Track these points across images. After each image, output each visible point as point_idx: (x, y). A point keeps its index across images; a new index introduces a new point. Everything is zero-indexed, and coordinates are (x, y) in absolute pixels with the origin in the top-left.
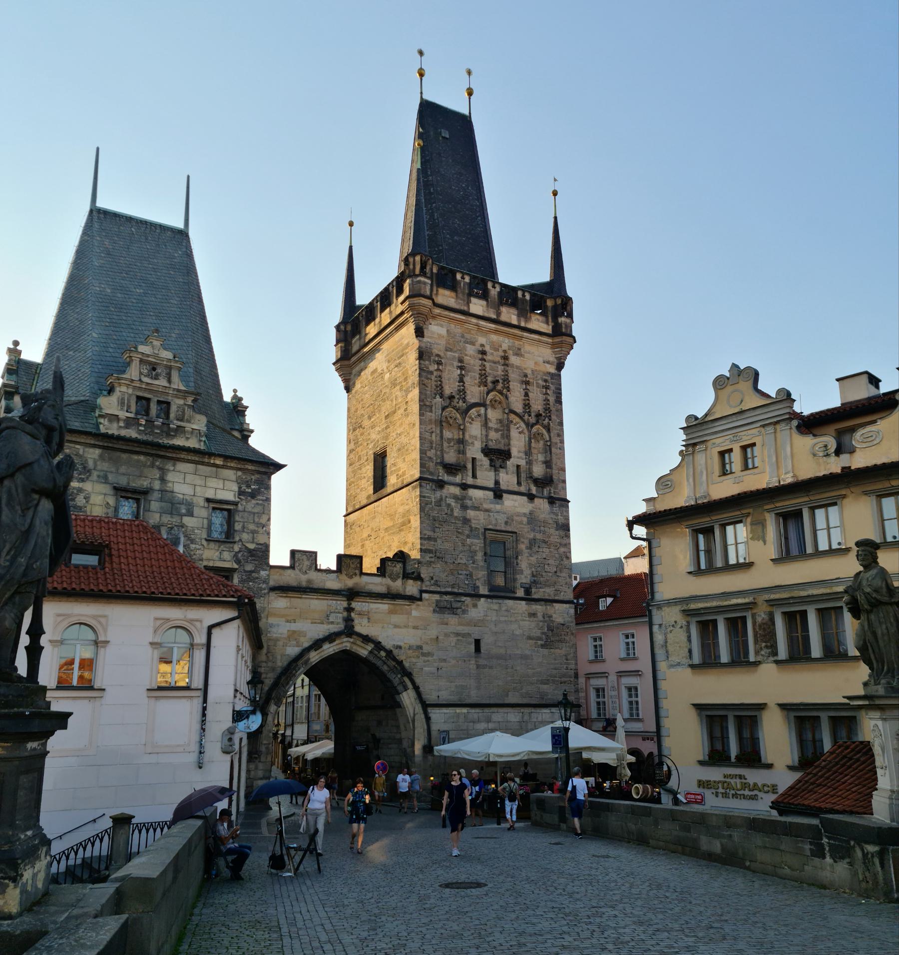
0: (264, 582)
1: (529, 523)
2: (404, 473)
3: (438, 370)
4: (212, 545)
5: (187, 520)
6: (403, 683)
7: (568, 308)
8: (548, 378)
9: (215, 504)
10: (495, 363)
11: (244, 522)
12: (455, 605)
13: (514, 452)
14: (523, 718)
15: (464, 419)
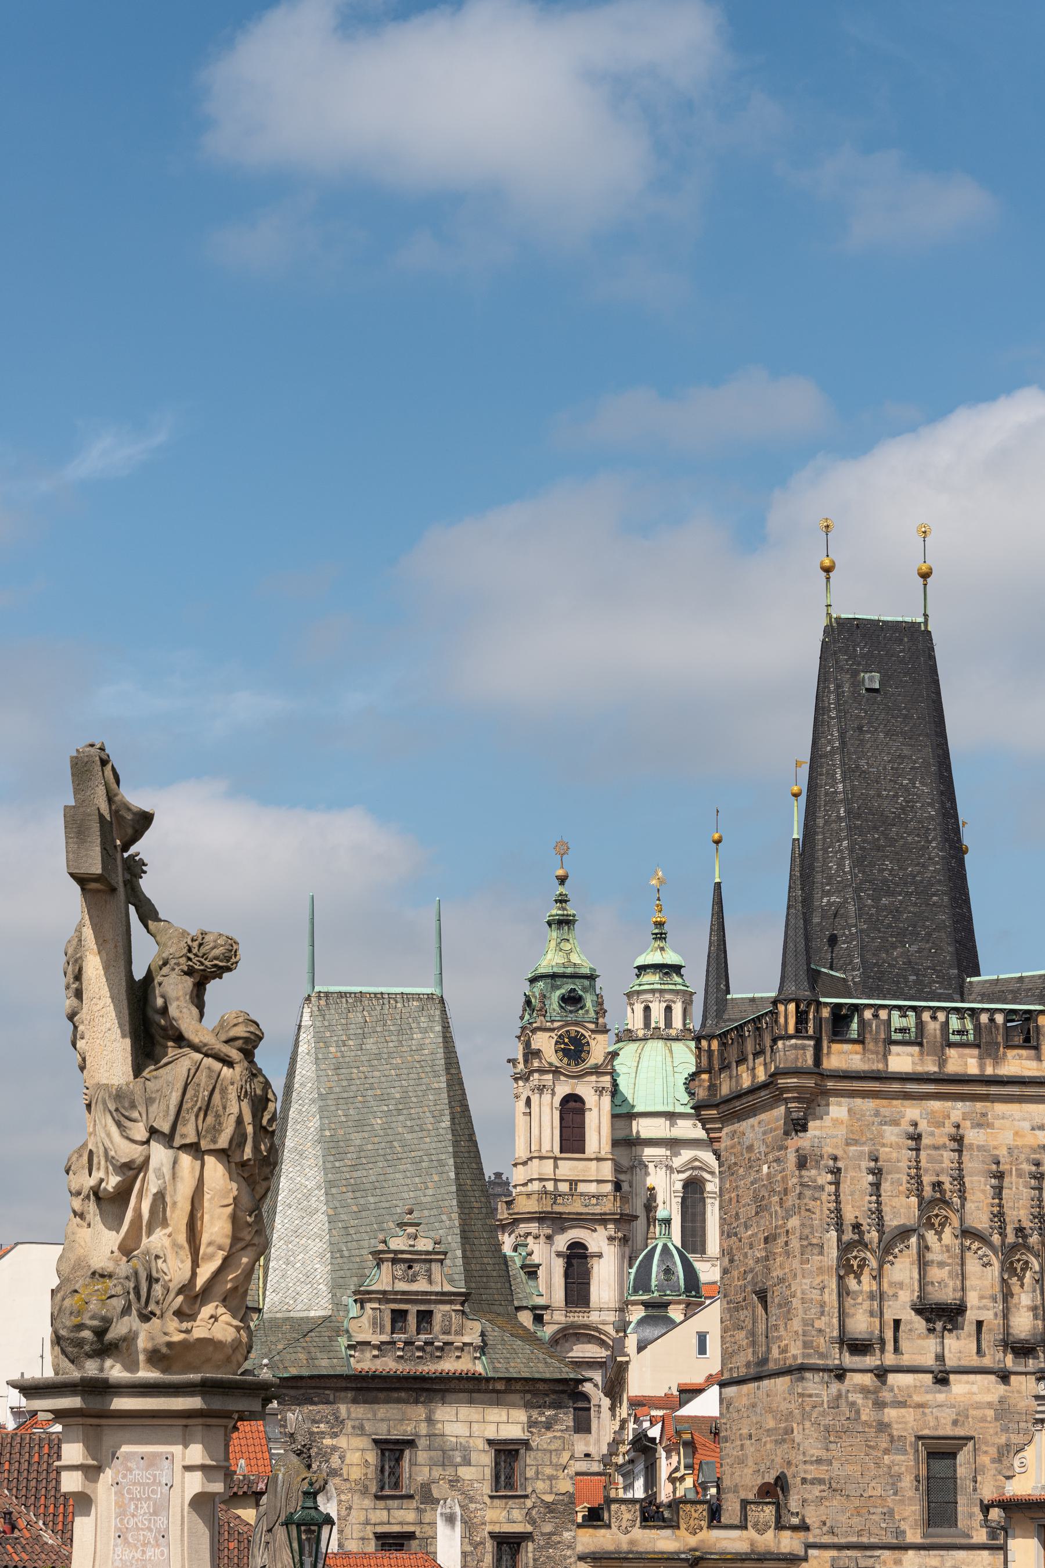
0: (569, 1547)
1: (996, 1419)
4: (497, 1502)
10: (936, 1148)
11: (537, 1465)
13: (972, 1299)
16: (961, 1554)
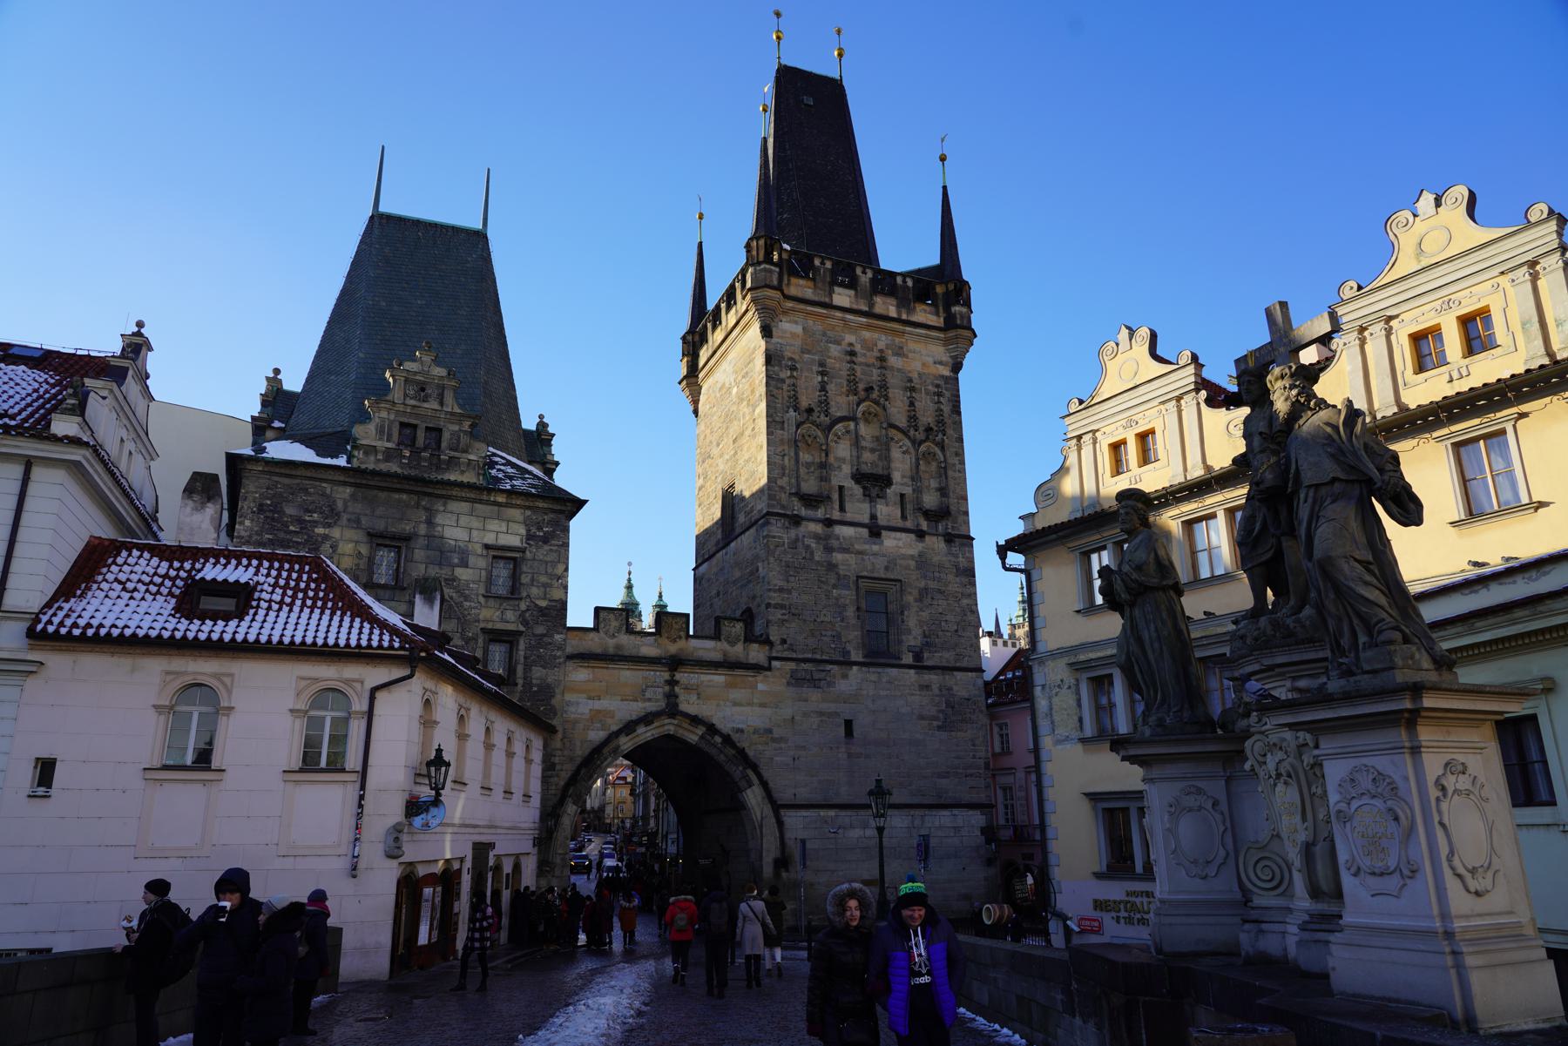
0: (559, 649)
2: (752, 510)
3: (792, 376)
4: (491, 602)
5: (459, 572)
6: (745, 777)
7: (964, 294)
8: (941, 383)
9: (497, 553)
10: (868, 366)
12: (816, 676)
13: (897, 477)
14: (913, 822)
15: (827, 437)
16: (893, 672)
